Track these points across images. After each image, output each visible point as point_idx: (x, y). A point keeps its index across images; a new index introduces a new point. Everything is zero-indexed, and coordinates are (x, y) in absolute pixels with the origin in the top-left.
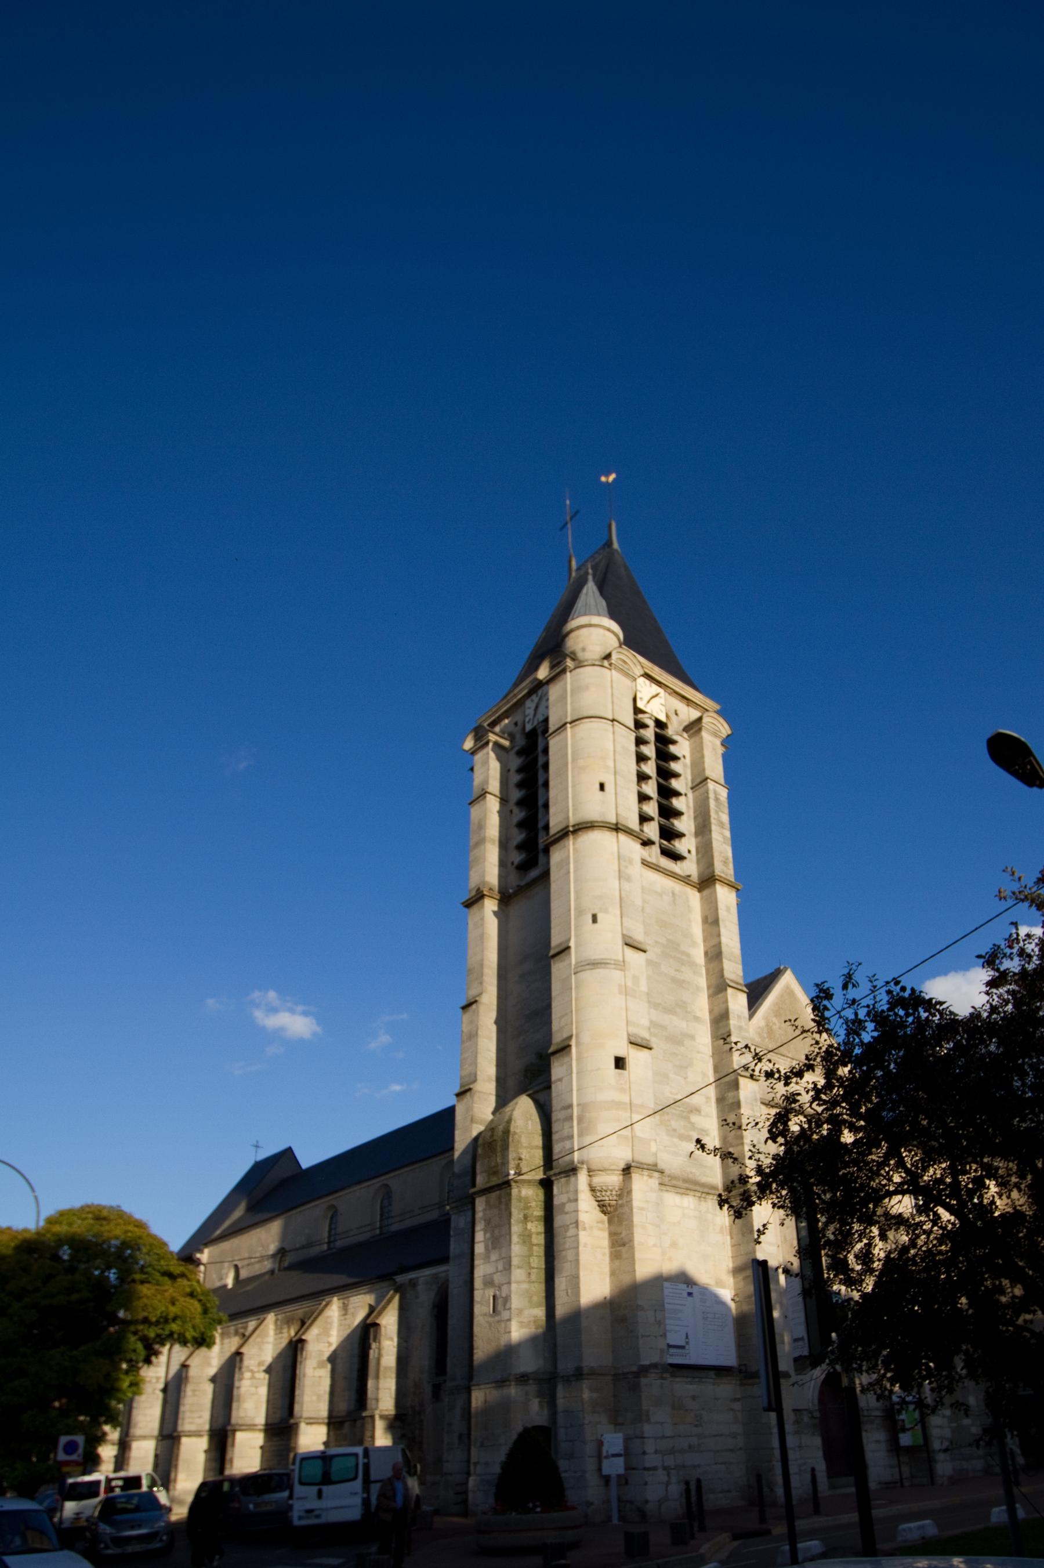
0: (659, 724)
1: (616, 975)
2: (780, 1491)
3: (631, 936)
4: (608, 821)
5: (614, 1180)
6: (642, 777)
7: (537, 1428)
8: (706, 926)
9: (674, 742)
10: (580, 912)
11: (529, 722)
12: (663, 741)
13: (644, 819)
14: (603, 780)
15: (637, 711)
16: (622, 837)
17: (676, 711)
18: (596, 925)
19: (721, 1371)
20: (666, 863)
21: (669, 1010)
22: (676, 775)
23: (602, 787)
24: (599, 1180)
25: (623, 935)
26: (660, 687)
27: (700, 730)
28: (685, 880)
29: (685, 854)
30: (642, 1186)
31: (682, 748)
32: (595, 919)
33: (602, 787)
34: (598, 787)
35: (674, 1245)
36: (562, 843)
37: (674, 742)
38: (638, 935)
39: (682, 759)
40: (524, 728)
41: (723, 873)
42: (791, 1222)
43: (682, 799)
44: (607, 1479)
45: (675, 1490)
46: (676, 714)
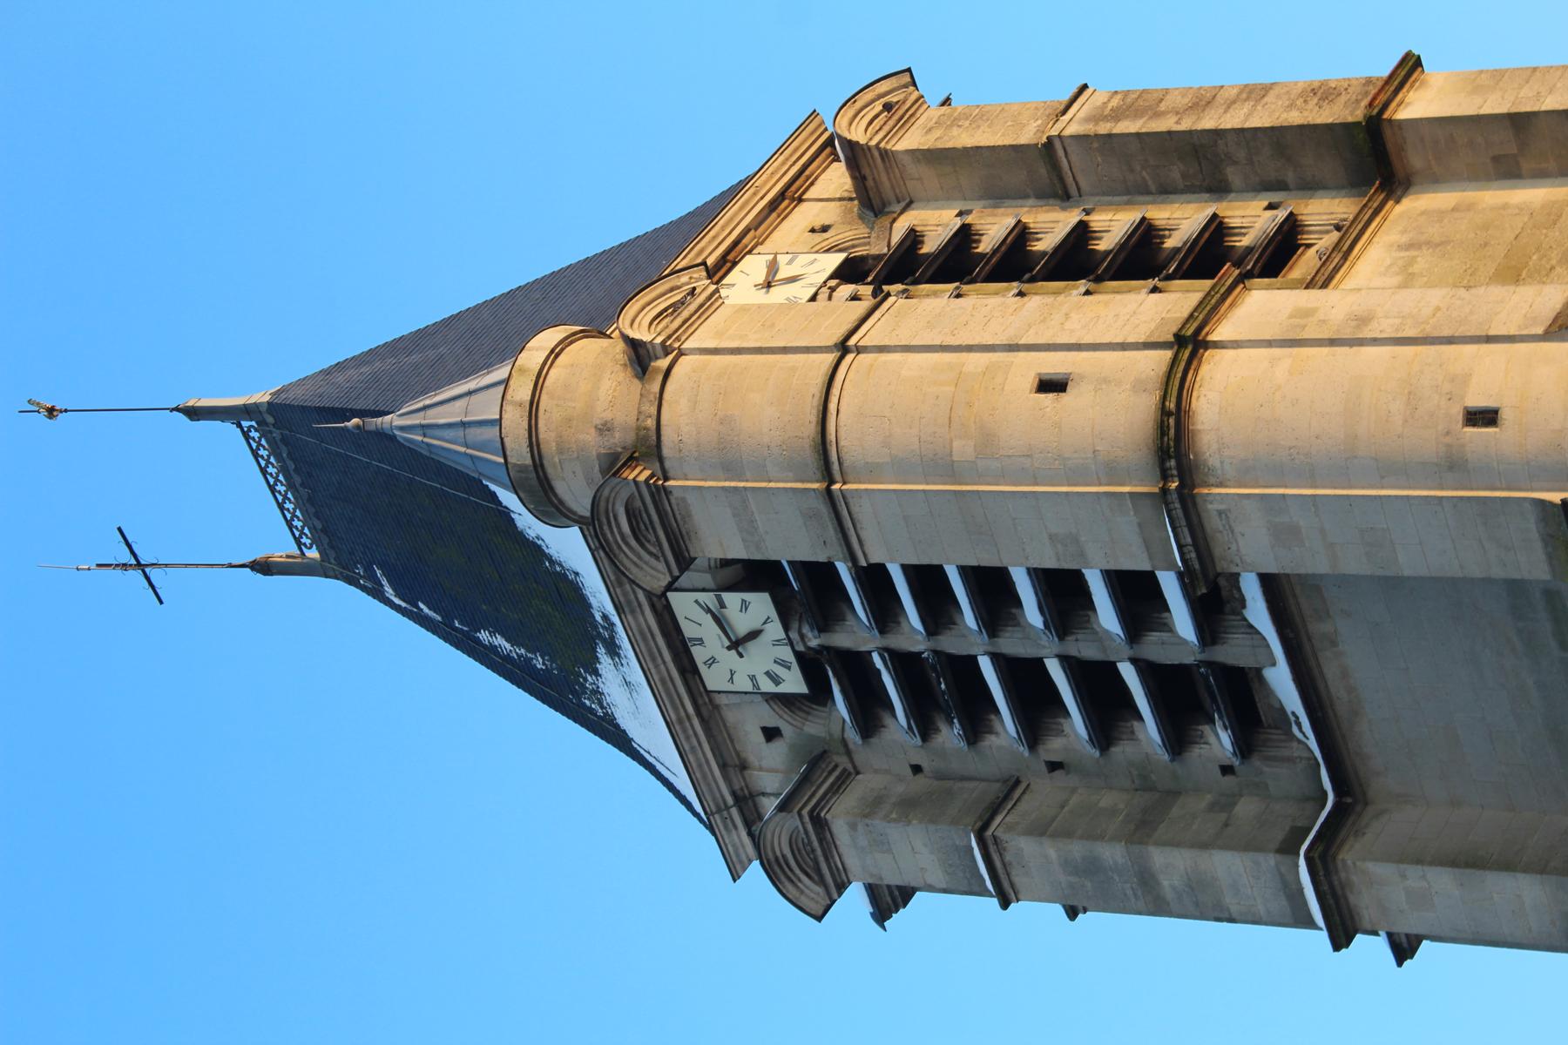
0: (850, 272)
3: (1552, 315)
4: (1164, 368)
8: (1526, 165)
9: (914, 238)
10: (1453, 466)
11: (776, 680)
14: (1031, 381)
16: (1221, 331)
17: (813, 231)
18: (1506, 415)
22: (1021, 235)
23: (1051, 385)
25: (1547, 336)
26: (735, 264)
27: (885, 155)
29: (1281, 214)
32: (1484, 417)
33: (1051, 385)
34: (1051, 396)
36: (1213, 523)
37: (914, 238)
39: (969, 219)
40: (786, 701)
41: (1358, 101)
43: (1098, 220)
46: (825, 229)
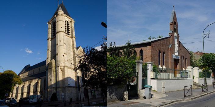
0: (67, 21)
1: (63, 47)
2: (80, 99)
5: (63, 68)
6: (66, 27)
7: (55, 93)
12: (68, 23)
13: (66, 31)
15: (65, 20)
19: (74, 87)
20: (68, 35)
21: (68, 50)
24: (61, 68)
28: (70, 37)
30: (65, 68)
31: (70, 24)
35: (69, 74)
38: (65, 43)
42: (81, 72)
44: (62, 98)
45: (69, 99)
